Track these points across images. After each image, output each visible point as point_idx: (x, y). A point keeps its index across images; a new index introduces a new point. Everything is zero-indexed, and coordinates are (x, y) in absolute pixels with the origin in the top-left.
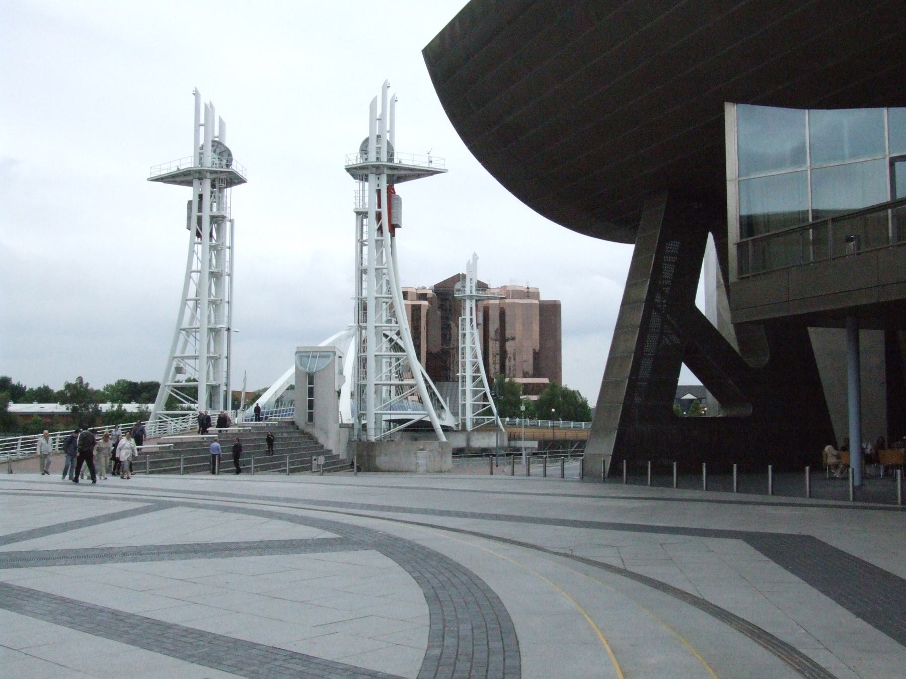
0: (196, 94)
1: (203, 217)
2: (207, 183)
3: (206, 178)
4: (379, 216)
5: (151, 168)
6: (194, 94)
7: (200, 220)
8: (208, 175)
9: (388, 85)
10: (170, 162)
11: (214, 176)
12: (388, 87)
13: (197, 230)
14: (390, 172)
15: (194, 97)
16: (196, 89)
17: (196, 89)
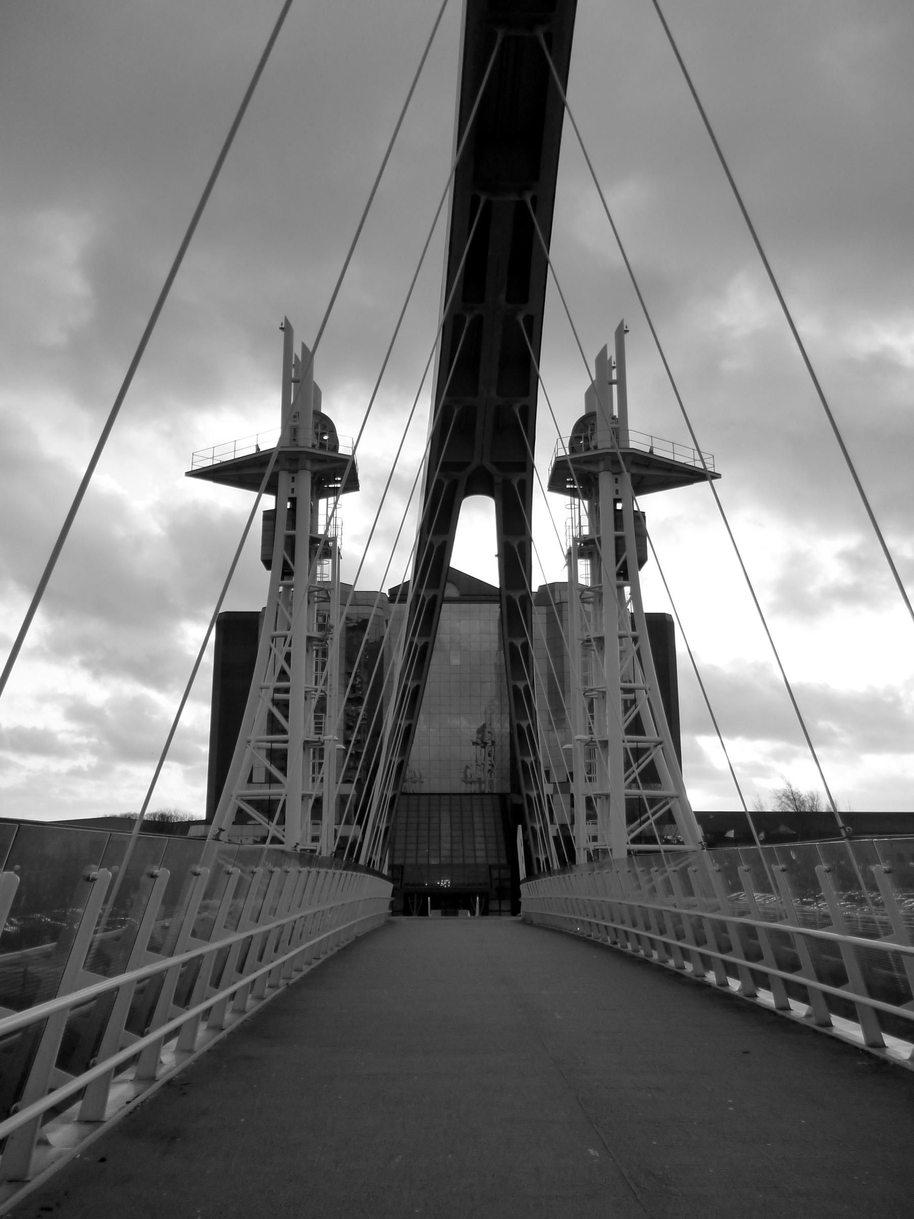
0: (287, 329)
1: (296, 536)
2: (305, 481)
3: (305, 469)
4: (620, 544)
5: (193, 454)
6: (281, 328)
7: (291, 544)
8: (308, 465)
9: (625, 329)
10: (235, 441)
11: (317, 467)
12: (628, 331)
13: (285, 563)
14: (634, 470)
15: (282, 333)
16: (286, 320)
17: (286, 320)
